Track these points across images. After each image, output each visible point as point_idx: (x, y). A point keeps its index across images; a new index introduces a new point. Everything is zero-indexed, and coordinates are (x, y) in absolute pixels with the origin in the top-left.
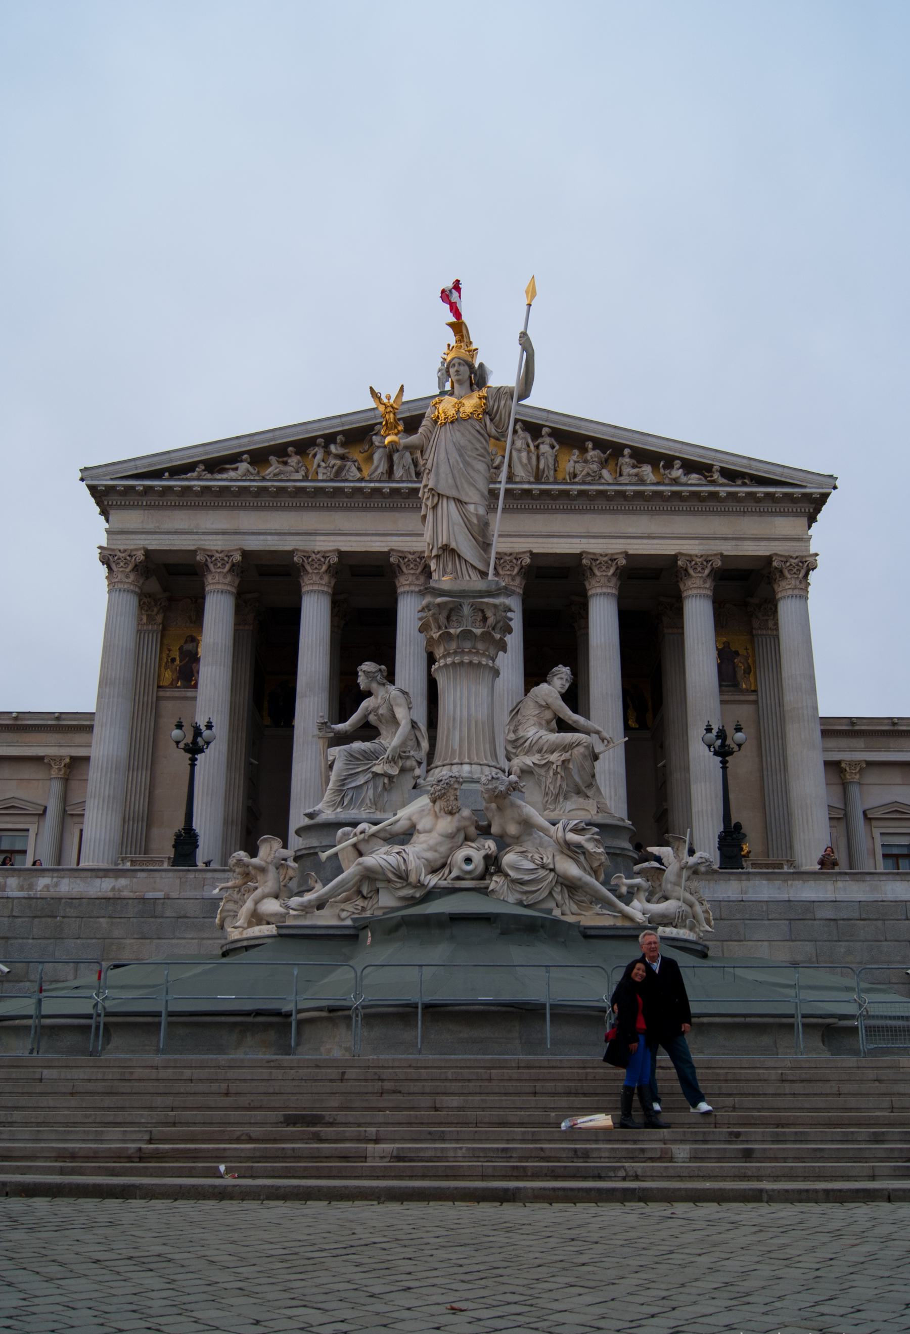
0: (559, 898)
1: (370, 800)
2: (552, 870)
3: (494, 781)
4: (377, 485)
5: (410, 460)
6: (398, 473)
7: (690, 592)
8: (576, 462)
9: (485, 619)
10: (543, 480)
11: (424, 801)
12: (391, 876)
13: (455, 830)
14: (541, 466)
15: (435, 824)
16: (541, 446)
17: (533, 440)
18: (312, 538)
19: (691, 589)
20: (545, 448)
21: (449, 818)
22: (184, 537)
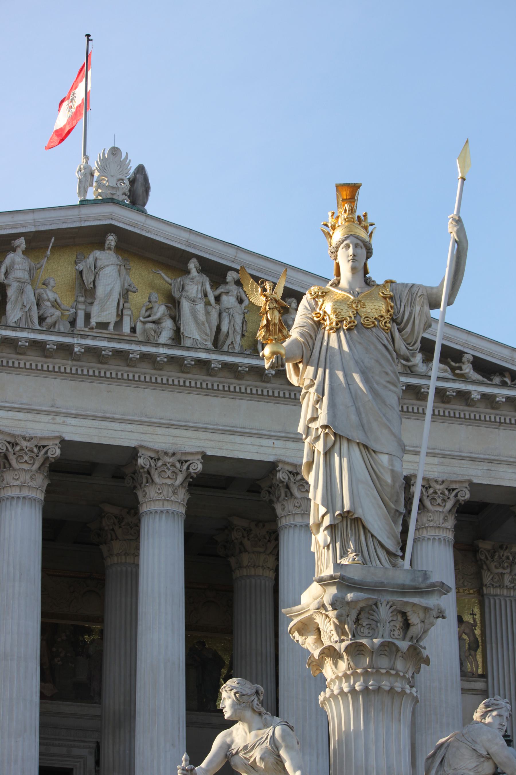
5: (33, 299)
9: (407, 625)
10: (225, 348)
14: (224, 328)
16: (224, 298)
17: (212, 287)
19: (426, 528)
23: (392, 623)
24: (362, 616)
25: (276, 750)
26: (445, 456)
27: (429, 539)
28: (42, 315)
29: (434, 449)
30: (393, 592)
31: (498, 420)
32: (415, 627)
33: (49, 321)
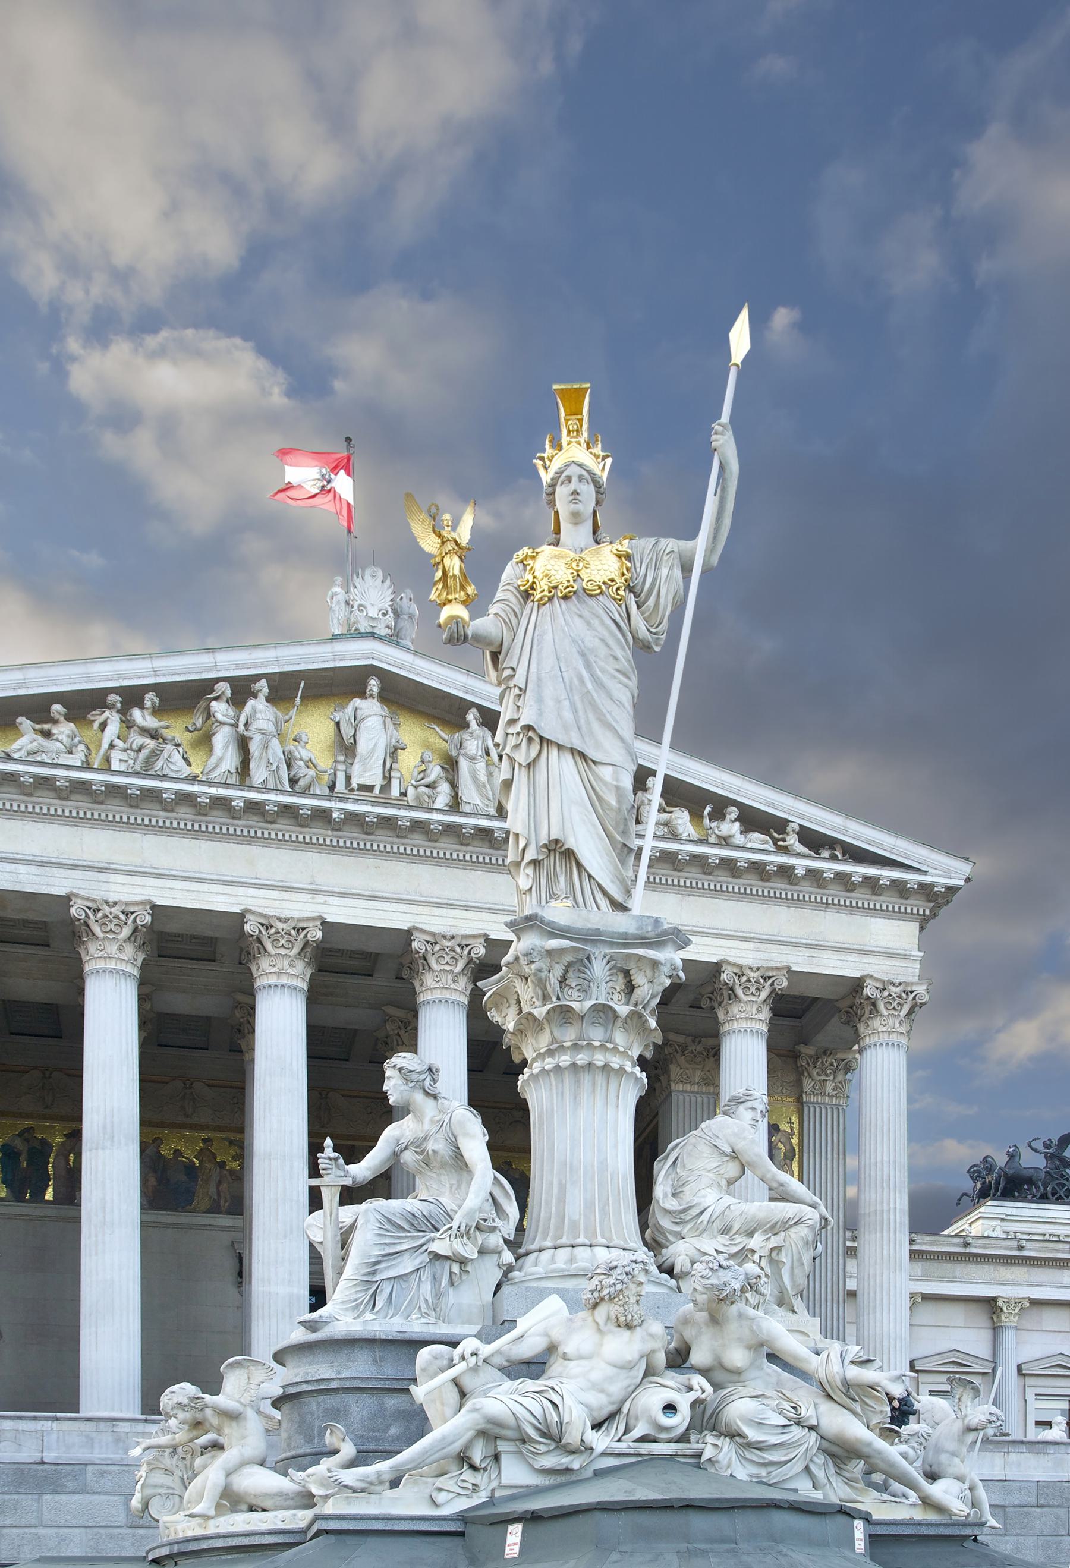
1: (426, 1300)
4: (222, 792)
6: (259, 773)
7: (735, 1025)
9: (630, 988)
11: (554, 1304)
13: (636, 1356)
15: (601, 1345)
21: (626, 1334)
23: (610, 984)
24: (570, 974)
25: (453, 1139)
26: (762, 941)
27: (740, 1031)
28: (294, 776)
29: (750, 933)
30: (612, 944)
31: (824, 901)
32: (641, 989)
33: (302, 782)
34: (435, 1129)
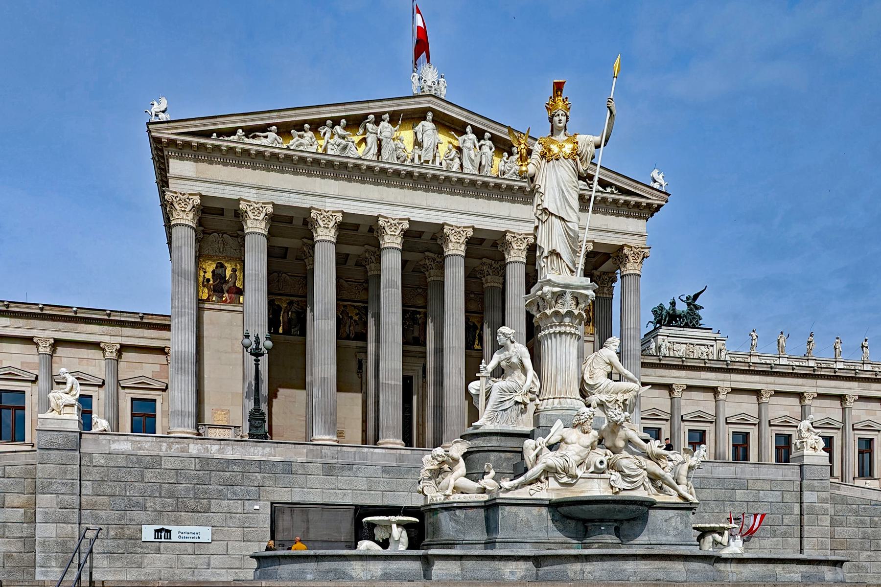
0: (647, 485)
2: (645, 469)
3: (618, 415)
6: (385, 155)
8: (505, 163)
12: (560, 470)
14: (483, 163)
18: (323, 199)
20: (486, 149)
22: (228, 187)
34: (514, 354)
